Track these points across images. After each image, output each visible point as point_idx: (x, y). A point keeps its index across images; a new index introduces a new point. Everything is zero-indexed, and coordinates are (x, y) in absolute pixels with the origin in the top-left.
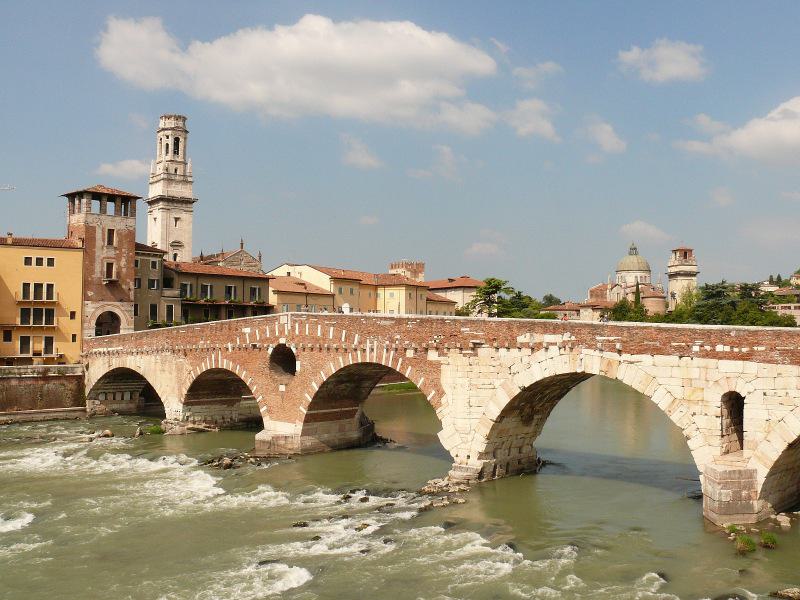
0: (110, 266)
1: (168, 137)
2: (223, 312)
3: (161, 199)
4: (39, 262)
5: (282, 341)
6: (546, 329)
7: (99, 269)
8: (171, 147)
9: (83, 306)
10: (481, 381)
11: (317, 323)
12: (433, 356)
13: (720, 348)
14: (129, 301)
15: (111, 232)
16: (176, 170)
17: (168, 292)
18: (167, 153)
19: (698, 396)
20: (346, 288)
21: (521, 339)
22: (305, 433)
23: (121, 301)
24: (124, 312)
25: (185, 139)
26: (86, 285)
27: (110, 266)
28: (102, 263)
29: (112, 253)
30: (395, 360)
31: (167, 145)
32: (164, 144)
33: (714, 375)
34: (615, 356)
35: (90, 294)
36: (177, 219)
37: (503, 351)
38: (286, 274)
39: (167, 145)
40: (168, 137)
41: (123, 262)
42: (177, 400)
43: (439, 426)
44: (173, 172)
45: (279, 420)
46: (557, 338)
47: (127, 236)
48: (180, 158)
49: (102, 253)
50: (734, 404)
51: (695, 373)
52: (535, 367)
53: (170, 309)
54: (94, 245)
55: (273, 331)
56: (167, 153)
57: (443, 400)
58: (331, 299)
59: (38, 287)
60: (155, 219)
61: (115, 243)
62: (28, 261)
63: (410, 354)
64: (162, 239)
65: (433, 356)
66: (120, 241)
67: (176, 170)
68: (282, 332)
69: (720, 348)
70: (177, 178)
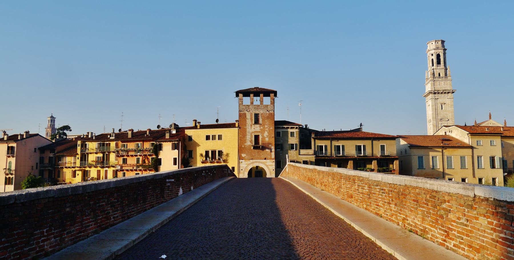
0: (257, 137)
1: (432, 55)
2: (351, 163)
4: (214, 137)
7: (249, 142)
8: (435, 61)
9: (239, 163)
14: (271, 159)
15: (257, 116)
17: (303, 151)
18: (433, 65)
20: (485, 141)
23: (265, 159)
25: (444, 54)
26: (240, 150)
27: (257, 137)
28: (251, 134)
29: (257, 128)
31: (433, 60)
32: (431, 60)
35: (243, 155)
38: (444, 134)
39: (433, 60)
40: (432, 55)
41: (266, 134)
44: (438, 75)
47: (268, 118)
49: (252, 129)
54: (245, 125)
58: (470, 151)
59: (213, 152)
61: (261, 121)
62: (208, 138)
64: (433, 118)
66: (263, 120)
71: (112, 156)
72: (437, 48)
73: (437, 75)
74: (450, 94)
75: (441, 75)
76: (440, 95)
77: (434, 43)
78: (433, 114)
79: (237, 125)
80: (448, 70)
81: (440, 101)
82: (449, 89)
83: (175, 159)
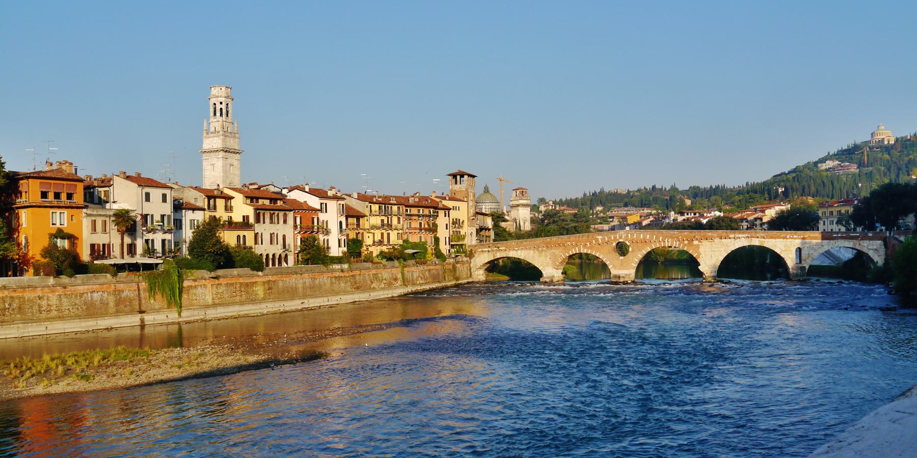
1: (221, 103)
5: (620, 241)
6: (740, 233)
8: (224, 111)
10: (717, 249)
11: (640, 234)
12: (696, 242)
13: (795, 236)
19: (789, 249)
21: (732, 236)
30: (679, 245)
31: (221, 109)
33: (793, 244)
34: (763, 240)
37: (724, 240)
39: (221, 109)
40: (221, 103)
42: (551, 268)
43: (699, 264)
45: (620, 269)
46: (744, 236)
50: (799, 250)
51: (788, 243)
52: (736, 244)
56: (221, 115)
57: (701, 256)
59: (456, 219)
63: (686, 242)
65: (696, 242)
68: (620, 237)
69: (795, 236)
71: (395, 220)
72: (227, 97)
73: (225, 130)
74: (237, 155)
76: (229, 154)
77: (223, 89)
78: (223, 176)
79: (465, 200)
81: (229, 161)
82: (237, 148)
83: (447, 224)
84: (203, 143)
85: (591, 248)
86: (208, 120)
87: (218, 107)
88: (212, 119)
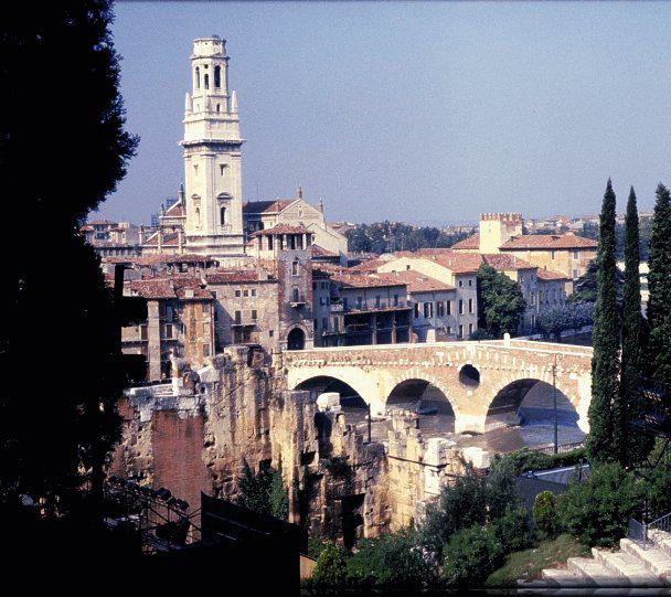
1: (206, 66)
3: (206, 144)
5: (468, 363)
16: (218, 106)
22: (487, 422)
24: (307, 326)
25: (227, 66)
31: (207, 76)
36: (223, 166)
39: (207, 76)
40: (206, 66)
48: (222, 92)
53: (336, 320)
55: (461, 356)
60: (196, 167)
62: (238, 294)
67: (218, 106)
70: (221, 117)
75: (221, 110)
80: (233, 99)
84: (183, 132)
85: (426, 371)
86: (191, 94)
87: (203, 72)
88: (195, 94)
